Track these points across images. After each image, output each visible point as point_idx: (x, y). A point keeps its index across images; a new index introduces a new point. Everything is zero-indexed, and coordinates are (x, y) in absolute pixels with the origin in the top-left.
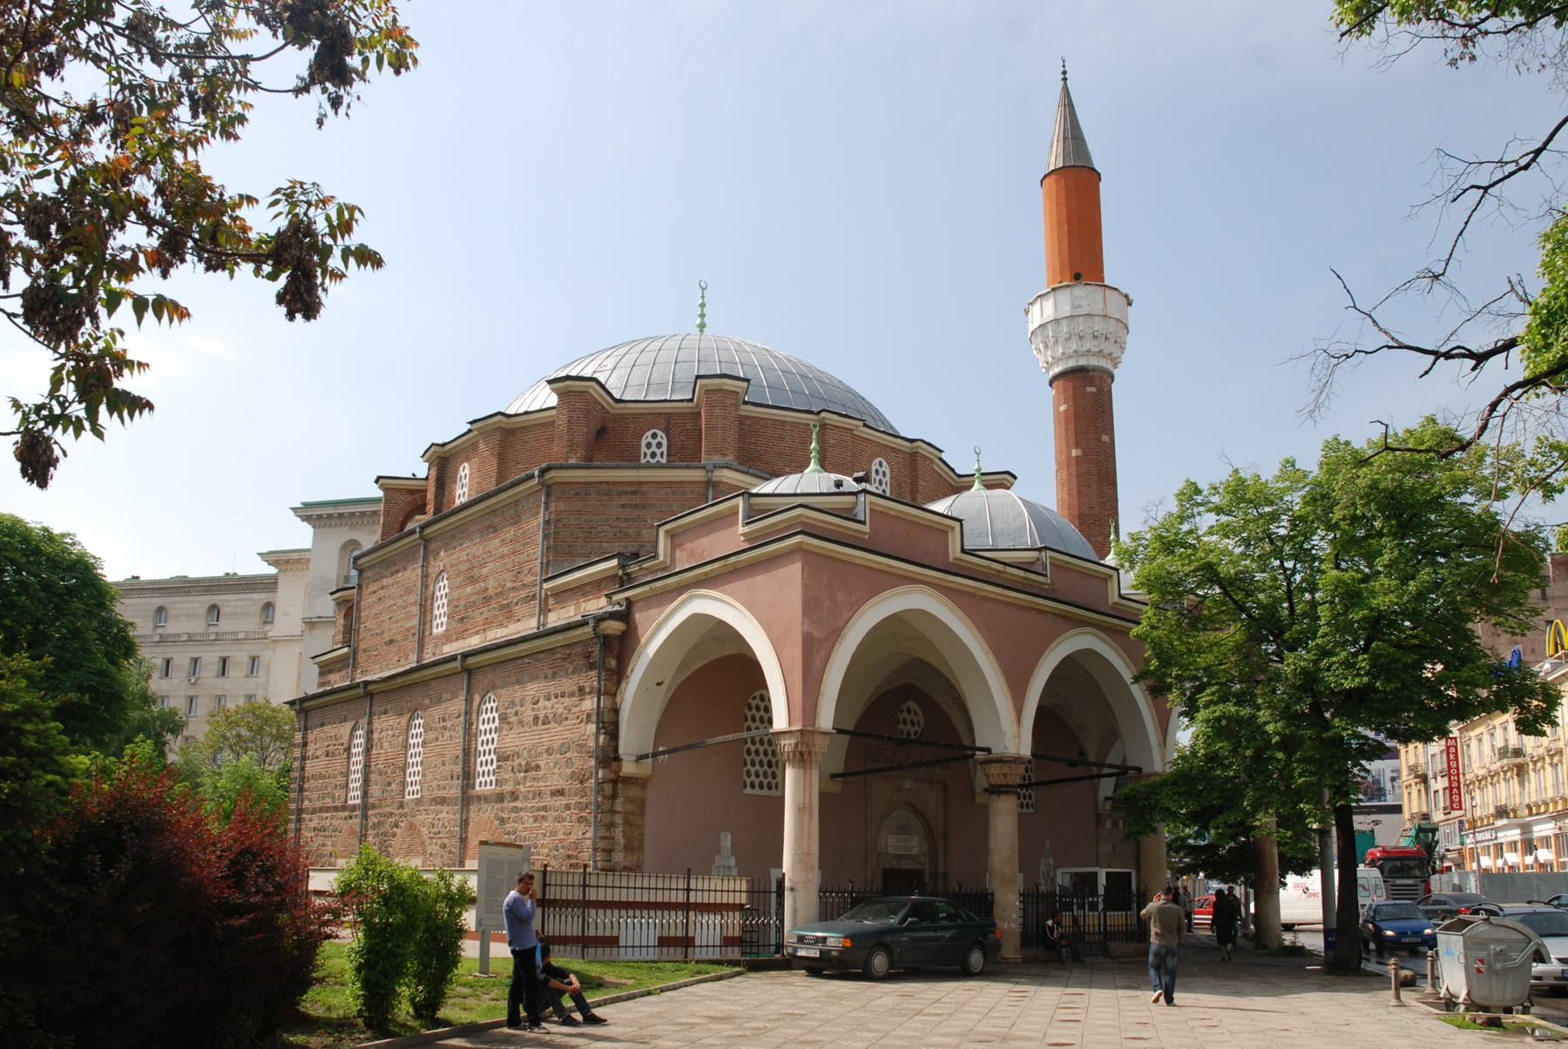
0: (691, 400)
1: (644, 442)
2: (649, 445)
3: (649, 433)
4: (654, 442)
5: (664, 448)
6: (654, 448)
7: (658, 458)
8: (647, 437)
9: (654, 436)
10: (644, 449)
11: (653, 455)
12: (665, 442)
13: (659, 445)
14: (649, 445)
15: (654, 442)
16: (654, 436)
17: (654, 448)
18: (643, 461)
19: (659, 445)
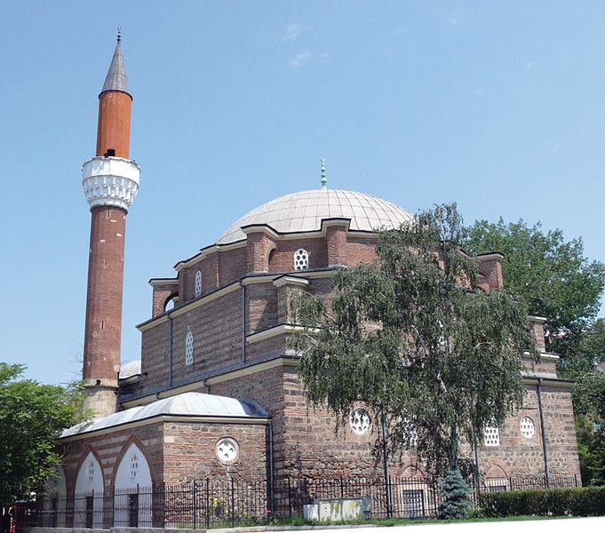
0: (321, 230)
1: (295, 256)
2: (298, 258)
3: (298, 252)
4: (301, 256)
5: (307, 259)
6: (301, 259)
7: (304, 264)
9: (301, 252)
10: (296, 260)
11: (301, 263)
12: (307, 256)
13: (304, 257)
14: (298, 258)
15: (301, 256)
17: (301, 259)
18: (296, 267)
19: (304, 257)
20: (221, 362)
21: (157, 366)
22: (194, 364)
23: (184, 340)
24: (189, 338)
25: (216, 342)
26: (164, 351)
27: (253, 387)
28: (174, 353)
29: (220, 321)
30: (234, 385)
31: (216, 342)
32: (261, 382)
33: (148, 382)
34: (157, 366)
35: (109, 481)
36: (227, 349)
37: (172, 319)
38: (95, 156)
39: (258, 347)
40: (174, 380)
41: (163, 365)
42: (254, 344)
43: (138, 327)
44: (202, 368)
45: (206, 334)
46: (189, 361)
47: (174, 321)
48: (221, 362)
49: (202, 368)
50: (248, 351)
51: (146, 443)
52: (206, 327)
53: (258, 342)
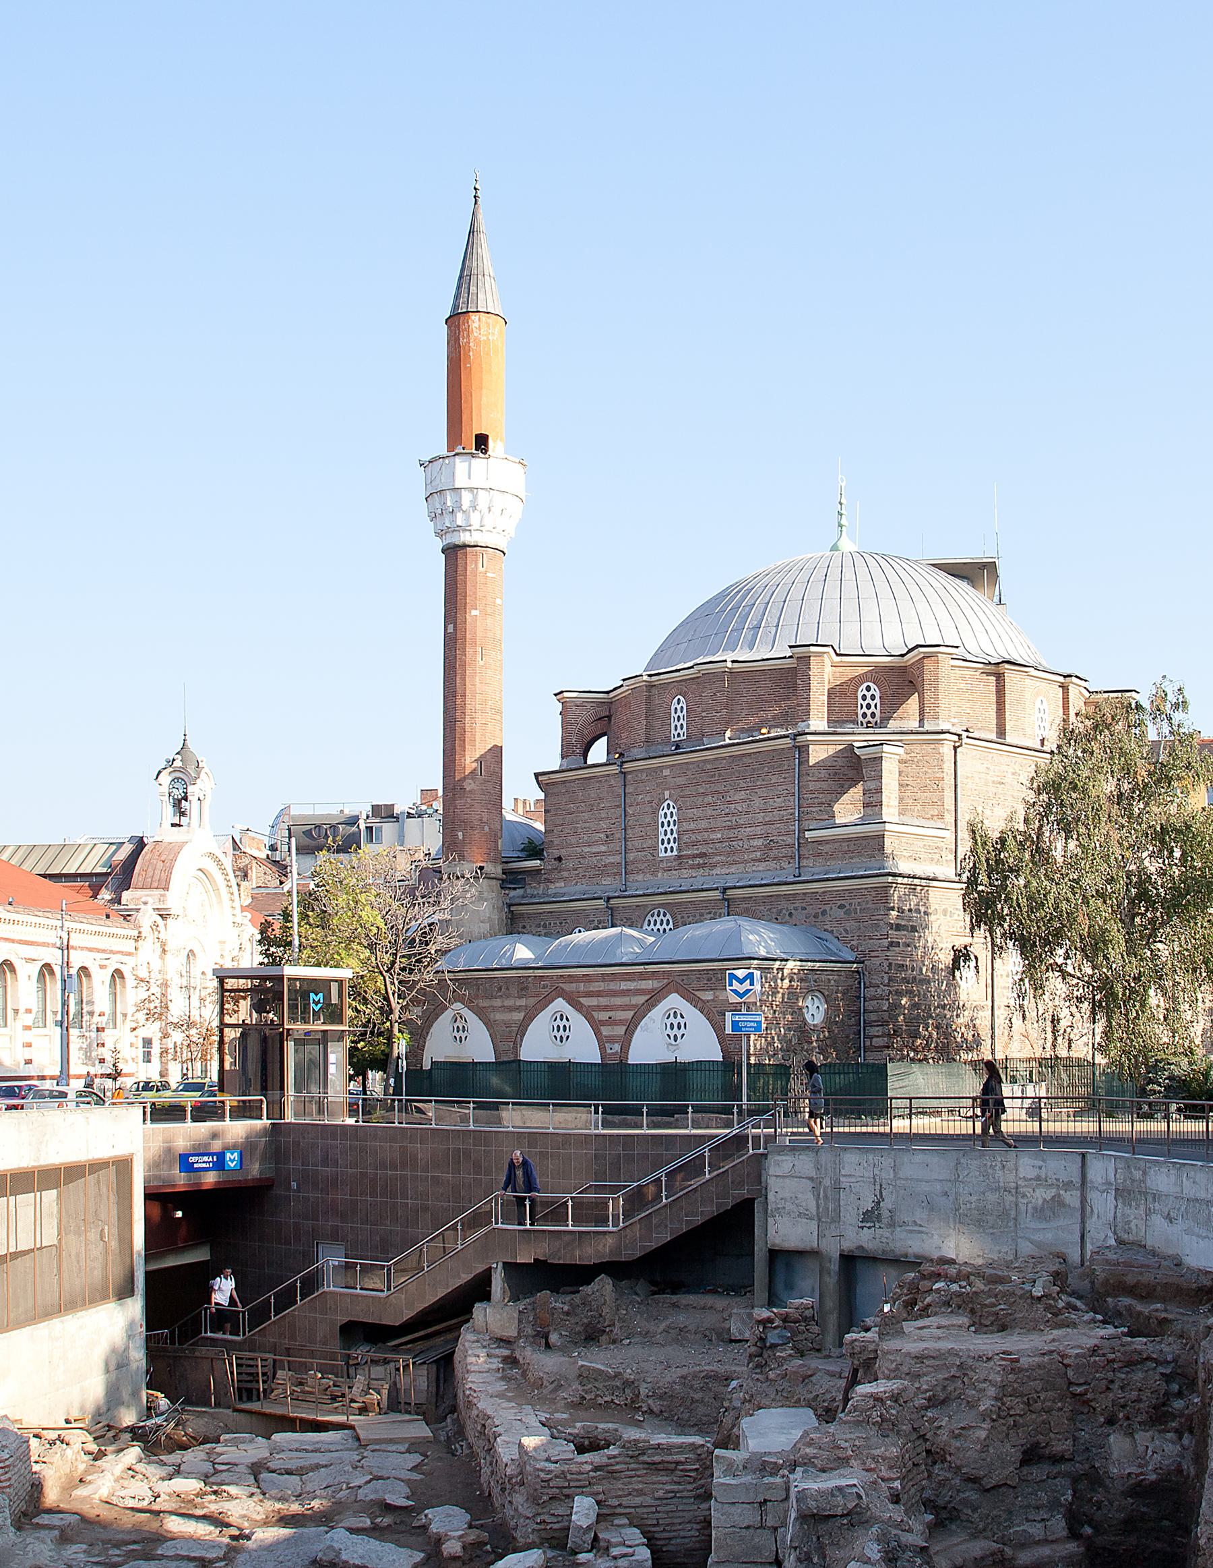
1: (860, 695)
4: (868, 695)
5: (877, 700)
6: (869, 700)
8: (862, 691)
9: (868, 688)
10: (860, 701)
12: (877, 695)
15: (868, 695)
16: (868, 688)
17: (869, 700)
18: (860, 712)
20: (746, 862)
21: (588, 849)
22: (679, 857)
23: (655, 813)
24: (668, 814)
25: (730, 828)
26: (603, 825)
27: (824, 913)
28: (629, 831)
29: (742, 795)
30: (784, 903)
31: (730, 828)
32: (841, 907)
33: (565, 874)
34: (588, 849)
35: (617, 1047)
36: (760, 842)
37: (625, 773)
38: (444, 452)
39: (826, 848)
40: (631, 877)
41: (603, 848)
42: (820, 843)
43: (537, 775)
44: (699, 866)
45: (709, 812)
46: (667, 849)
47: (629, 777)
48: (746, 862)
49: (699, 866)
50: (804, 851)
51: (708, 996)
52: (709, 799)
53: (827, 842)
